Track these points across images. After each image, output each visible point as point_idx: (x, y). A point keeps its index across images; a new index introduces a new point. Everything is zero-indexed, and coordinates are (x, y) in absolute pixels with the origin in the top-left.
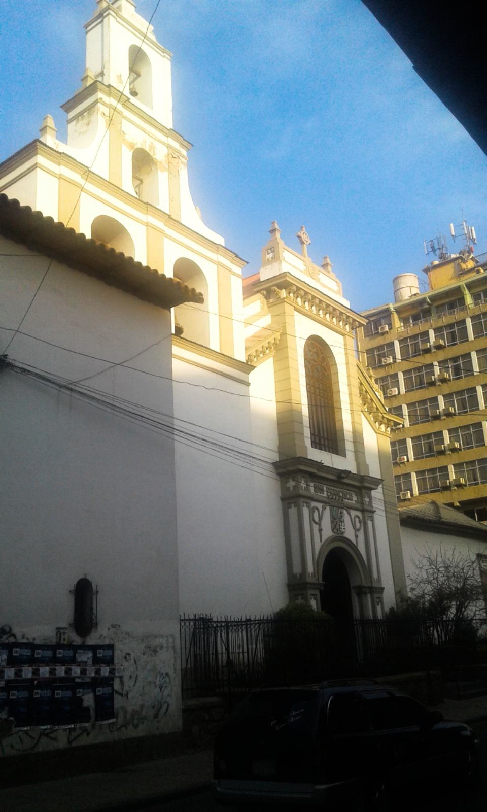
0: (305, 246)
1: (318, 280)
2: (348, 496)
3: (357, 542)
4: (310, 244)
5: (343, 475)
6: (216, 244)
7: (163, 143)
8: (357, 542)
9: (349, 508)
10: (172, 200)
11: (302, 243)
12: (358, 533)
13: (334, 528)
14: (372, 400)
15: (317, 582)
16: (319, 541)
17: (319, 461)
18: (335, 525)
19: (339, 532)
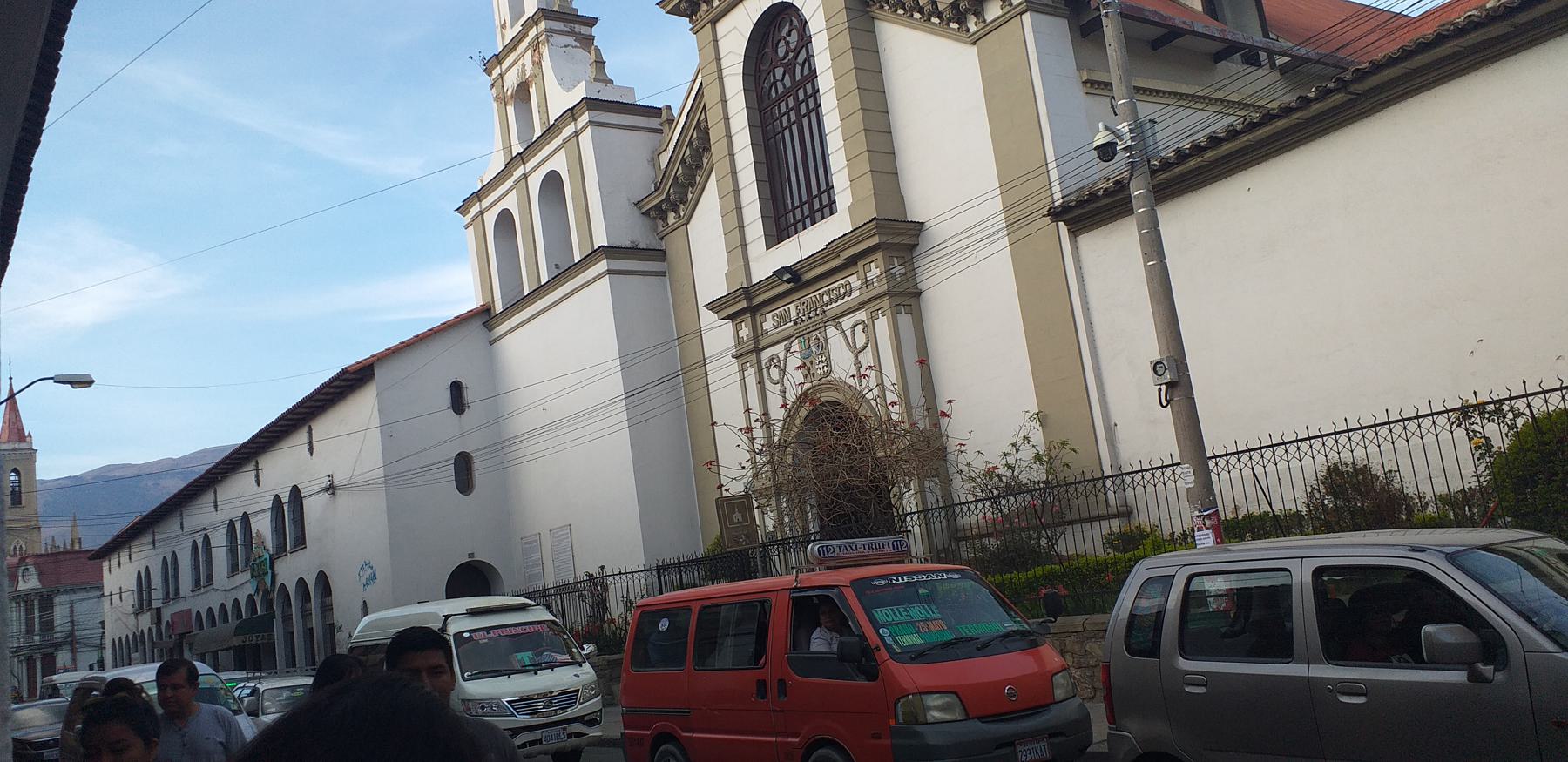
2: (842, 291)
18: (809, 369)
19: (817, 377)
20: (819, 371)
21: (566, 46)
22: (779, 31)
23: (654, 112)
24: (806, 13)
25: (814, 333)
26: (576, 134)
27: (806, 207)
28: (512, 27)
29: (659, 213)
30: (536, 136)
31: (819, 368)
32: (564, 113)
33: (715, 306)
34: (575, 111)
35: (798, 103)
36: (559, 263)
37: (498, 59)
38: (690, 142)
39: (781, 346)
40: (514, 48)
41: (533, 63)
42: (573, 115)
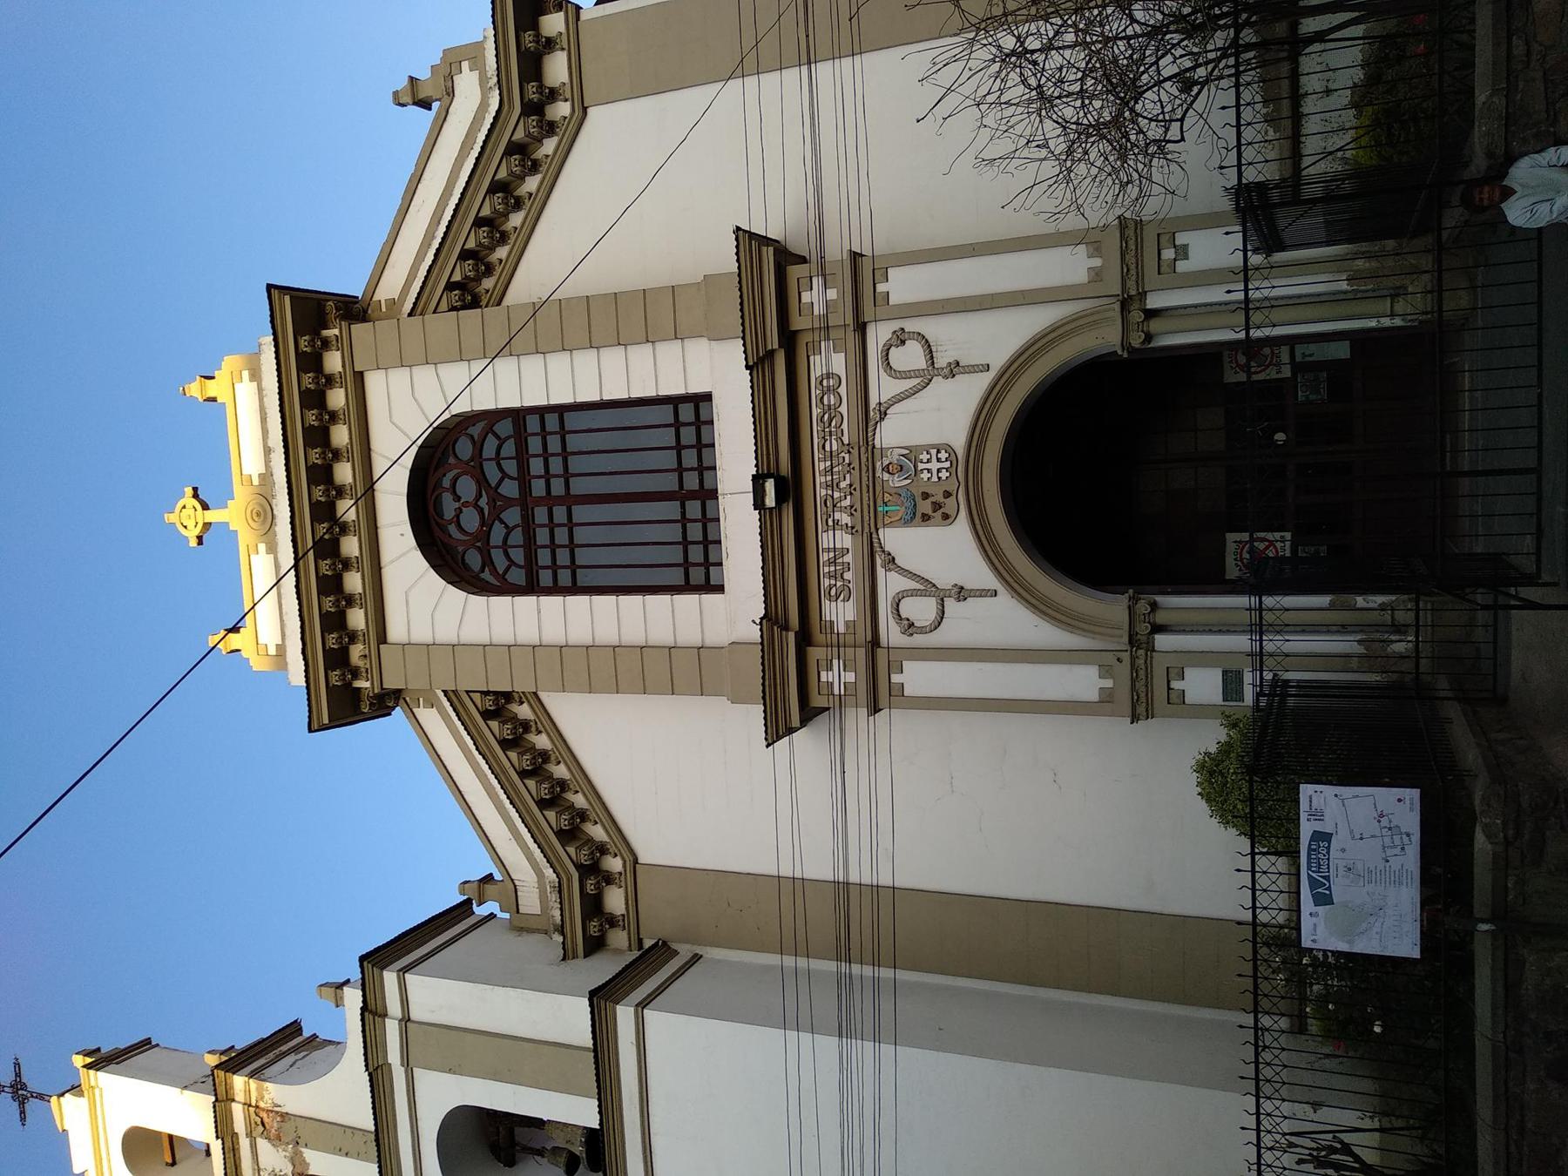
0: (212, 516)
4: (196, 496)
5: (770, 501)
6: (371, 1080)
9: (869, 417)
10: (347, 1154)
11: (207, 526)
12: (942, 361)
13: (946, 517)
15: (1126, 657)
17: (759, 627)
18: (937, 506)
20: (944, 474)
21: (291, 1066)
22: (443, 519)
23: (463, 909)
25: (877, 475)
26: (406, 1020)
27: (694, 509)
29: (593, 906)
31: (933, 469)
32: (364, 1031)
33: (777, 729)
34: (371, 1005)
35: (549, 500)
38: (523, 774)
39: (880, 571)
41: (277, 1140)
42: (375, 1014)
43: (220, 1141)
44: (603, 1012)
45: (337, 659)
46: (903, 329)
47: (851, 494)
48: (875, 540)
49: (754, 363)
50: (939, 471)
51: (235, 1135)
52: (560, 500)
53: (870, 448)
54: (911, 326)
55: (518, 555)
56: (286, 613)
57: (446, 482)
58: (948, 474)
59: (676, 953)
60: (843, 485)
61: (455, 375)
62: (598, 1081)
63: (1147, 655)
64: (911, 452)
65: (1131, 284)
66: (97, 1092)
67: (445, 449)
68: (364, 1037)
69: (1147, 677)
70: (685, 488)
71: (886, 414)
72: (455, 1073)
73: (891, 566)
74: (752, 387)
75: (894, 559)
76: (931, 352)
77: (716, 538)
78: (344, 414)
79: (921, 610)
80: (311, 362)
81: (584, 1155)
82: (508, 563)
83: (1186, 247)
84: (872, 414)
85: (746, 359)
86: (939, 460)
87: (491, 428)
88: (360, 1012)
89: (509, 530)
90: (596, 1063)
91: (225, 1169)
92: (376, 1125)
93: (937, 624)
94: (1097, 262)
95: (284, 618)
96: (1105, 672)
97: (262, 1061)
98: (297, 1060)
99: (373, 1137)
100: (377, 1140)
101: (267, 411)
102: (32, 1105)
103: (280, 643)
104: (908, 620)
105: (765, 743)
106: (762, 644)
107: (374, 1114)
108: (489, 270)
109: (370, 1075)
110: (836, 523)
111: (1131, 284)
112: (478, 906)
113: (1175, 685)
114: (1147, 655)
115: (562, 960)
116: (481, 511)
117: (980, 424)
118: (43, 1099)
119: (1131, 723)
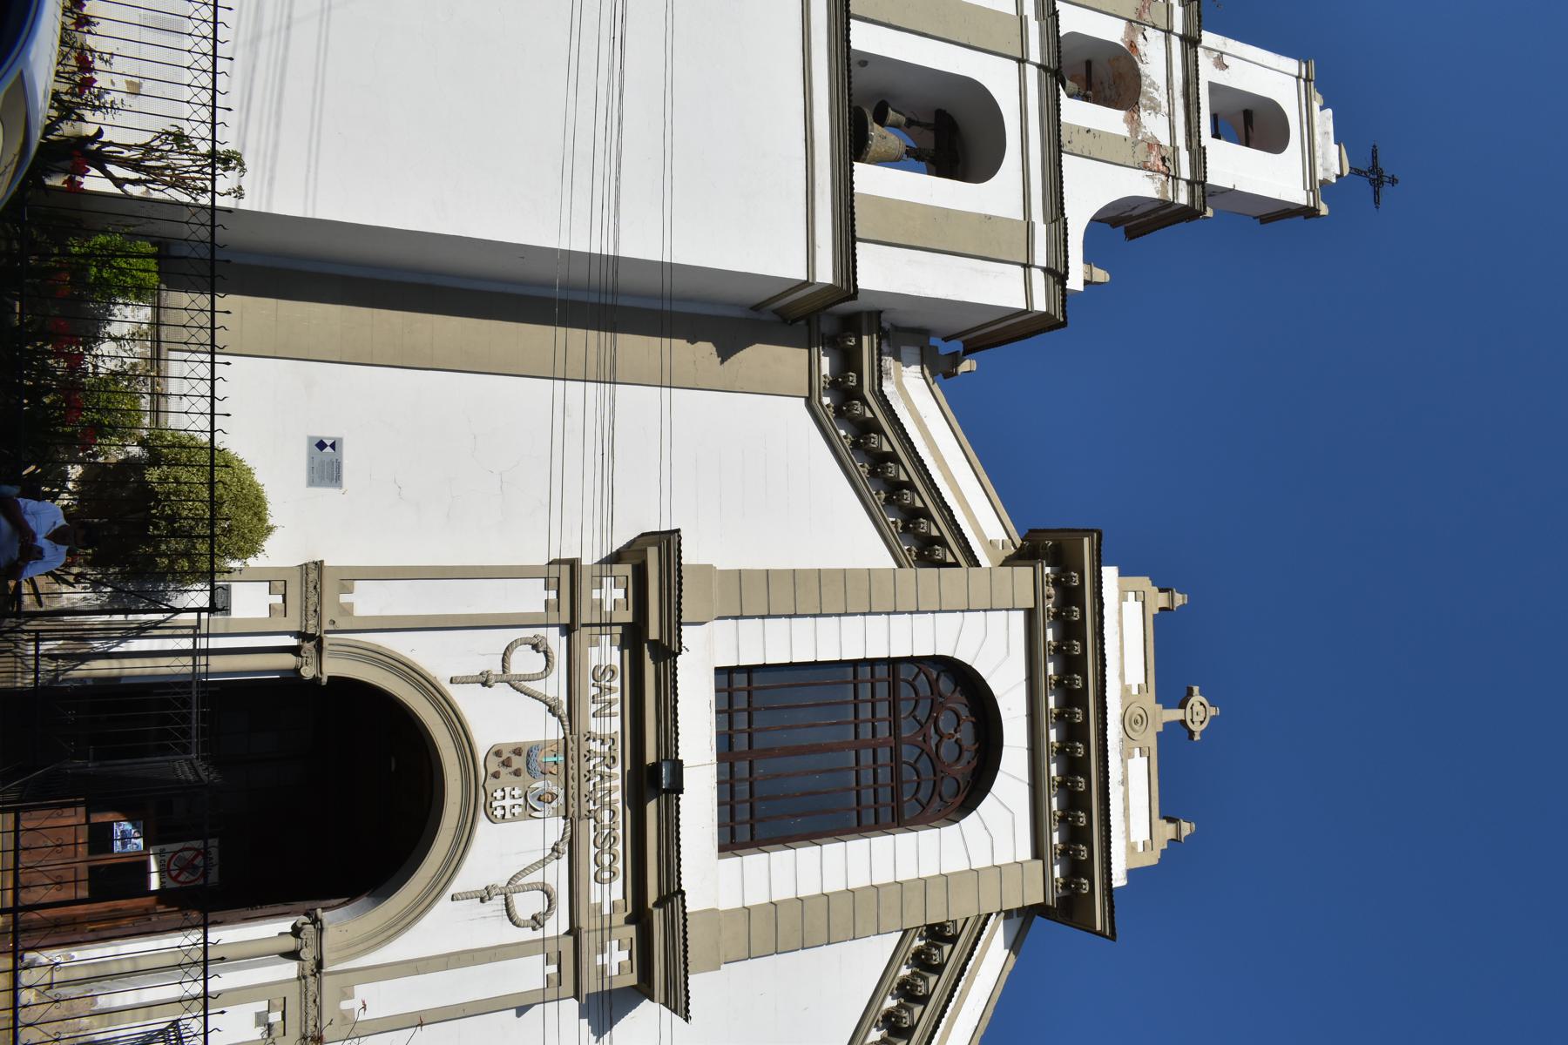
0: (1176, 715)
1: (1126, 756)
2: (606, 859)
3: (467, 896)
4: (1192, 733)
6: (1062, 209)
7: (1173, 137)
8: (467, 896)
10: (1088, 131)
11: (1183, 705)
12: (499, 901)
13: (498, 754)
14: (913, 1028)
15: (327, 626)
16: (454, 674)
18: (506, 763)
21: (1135, 208)
24: (970, 822)
25: (563, 790)
26: (1027, 266)
28: (1209, 82)
30: (1062, 92)
31: (508, 797)
32: (1066, 257)
36: (868, 66)
37: (1191, 42)
38: (910, 486)
39: (564, 697)
40: (1186, 94)
41: (1153, 144)
43: (1202, 146)
44: (845, 277)
45: (1069, 596)
46: (534, 929)
47: (589, 771)
48: (567, 727)
49: (677, 897)
50: (504, 798)
51: (1189, 148)
52: (866, 745)
53: (570, 816)
54: (527, 934)
55: (905, 691)
56: (1116, 633)
57: (967, 756)
58: (495, 795)
59: (775, 312)
60: (598, 778)
61: (955, 864)
62: (853, 213)
63: (306, 629)
64: (530, 815)
65: (313, 988)
66: (1308, 188)
67: (966, 787)
68: (1066, 251)
69: (306, 607)
70: (748, 762)
71: (553, 849)
72: (986, 216)
73: (553, 703)
74: (679, 873)
75: (550, 711)
76: (508, 910)
77: (721, 715)
78: (1054, 820)
79: (526, 662)
80: (1077, 869)
81: (870, 127)
82: (916, 683)
83: (258, 1024)
84: (567, 849)
85: (684, 901)
86: (504, 808)
87: (924, 808)
88: (1069, 276)
89: (912, 714)
90: (853, 225)
91: (1199, 118)
92: (1060, 161)
93: (510, 649)
94: (345, 1005)
95: (1118, 629)
96: (347, 610)
97: (1162, 212)
98: (1130, 211)
99: (1064, 149)
100: (1060, 146)
101: (1122, 818)
102: (1365, 165)
103: (1124, 603)
104: (538, 652)
105: (682, 534)
106: (680, 624)
107: (1061, 177)
108: (917, 954)
109: (1063, 215)
110: (603, 742)
111: (313, 988)
112: (958, 351)
113: (278, 599)
114: (306, 629)
115: (881, 312)
116: (937, 730)
117: (462, 846)
118: (1355, 169)
119: (322, 562)
